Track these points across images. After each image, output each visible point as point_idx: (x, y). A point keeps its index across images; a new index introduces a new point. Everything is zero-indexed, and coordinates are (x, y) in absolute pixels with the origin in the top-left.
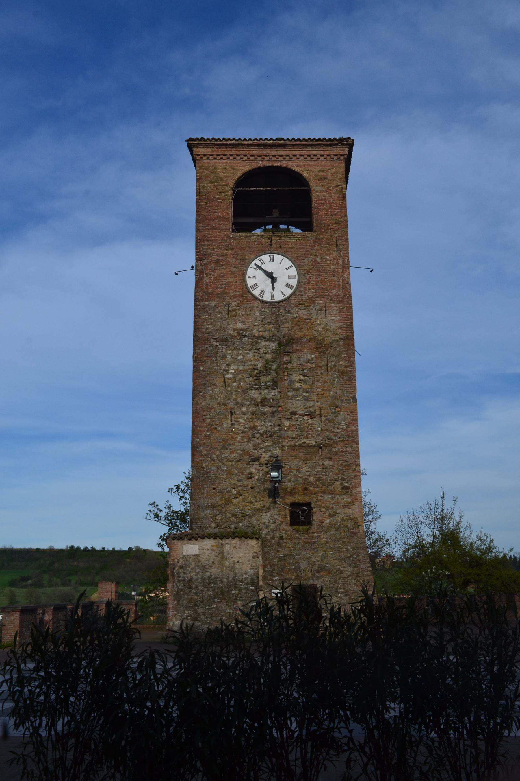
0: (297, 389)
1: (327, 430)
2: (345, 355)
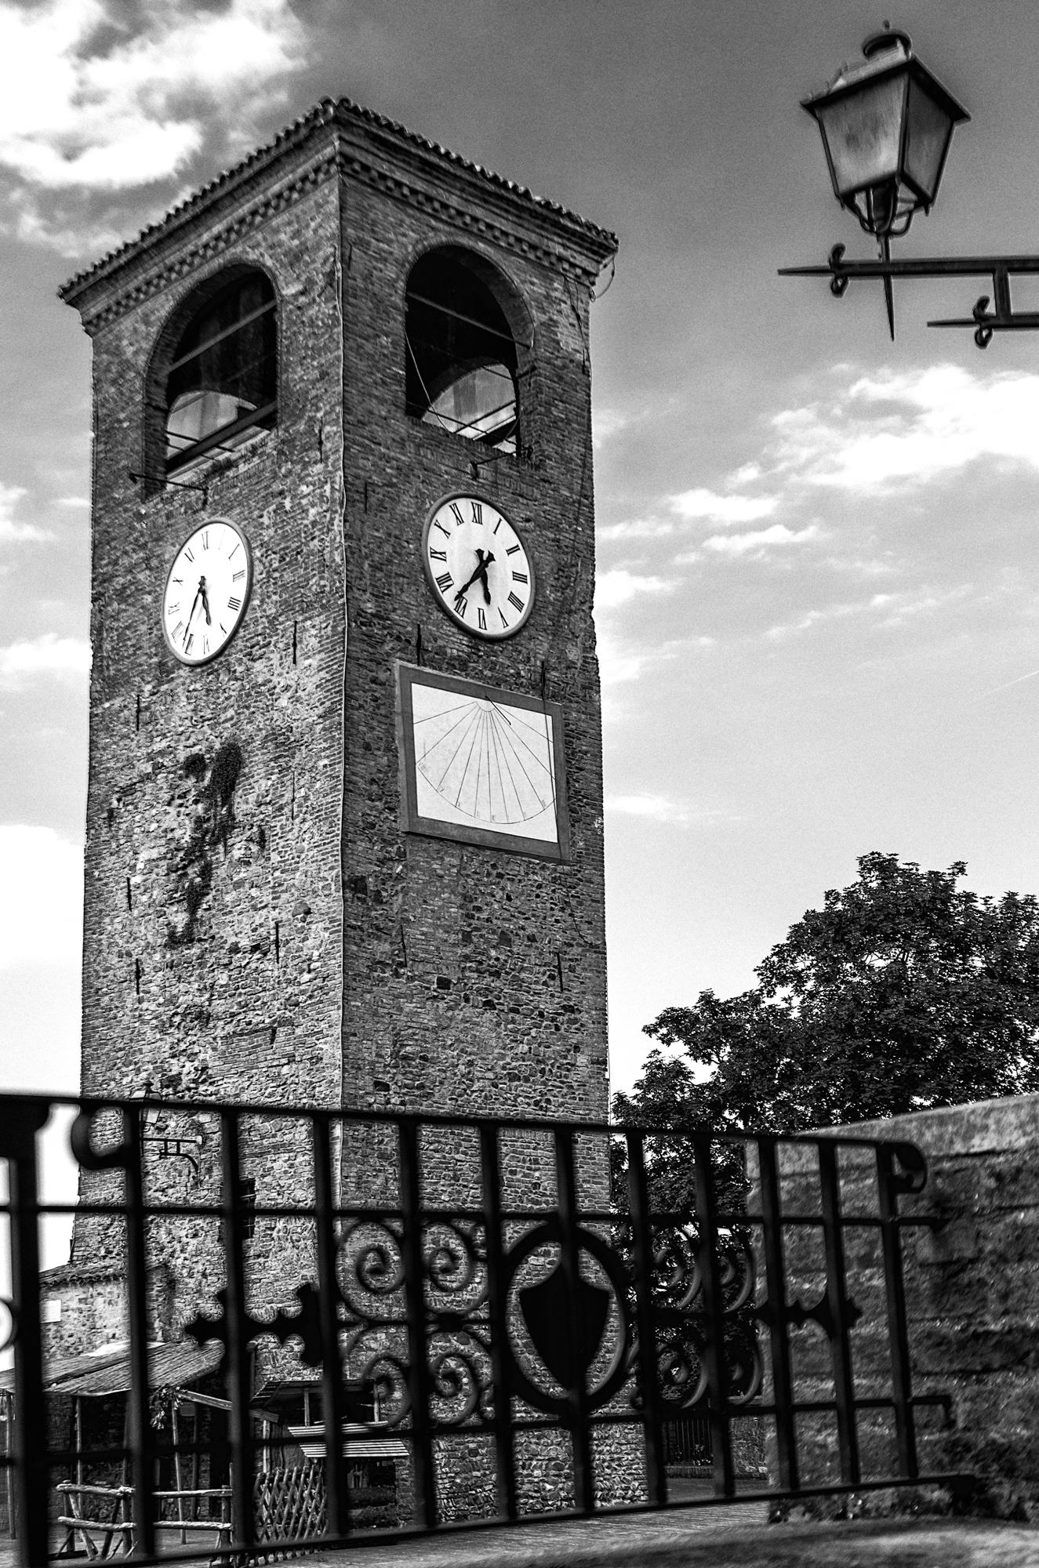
0: (238, 885)
1: (289, 982)
2: (326, 762)
